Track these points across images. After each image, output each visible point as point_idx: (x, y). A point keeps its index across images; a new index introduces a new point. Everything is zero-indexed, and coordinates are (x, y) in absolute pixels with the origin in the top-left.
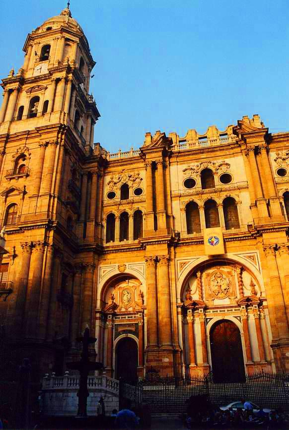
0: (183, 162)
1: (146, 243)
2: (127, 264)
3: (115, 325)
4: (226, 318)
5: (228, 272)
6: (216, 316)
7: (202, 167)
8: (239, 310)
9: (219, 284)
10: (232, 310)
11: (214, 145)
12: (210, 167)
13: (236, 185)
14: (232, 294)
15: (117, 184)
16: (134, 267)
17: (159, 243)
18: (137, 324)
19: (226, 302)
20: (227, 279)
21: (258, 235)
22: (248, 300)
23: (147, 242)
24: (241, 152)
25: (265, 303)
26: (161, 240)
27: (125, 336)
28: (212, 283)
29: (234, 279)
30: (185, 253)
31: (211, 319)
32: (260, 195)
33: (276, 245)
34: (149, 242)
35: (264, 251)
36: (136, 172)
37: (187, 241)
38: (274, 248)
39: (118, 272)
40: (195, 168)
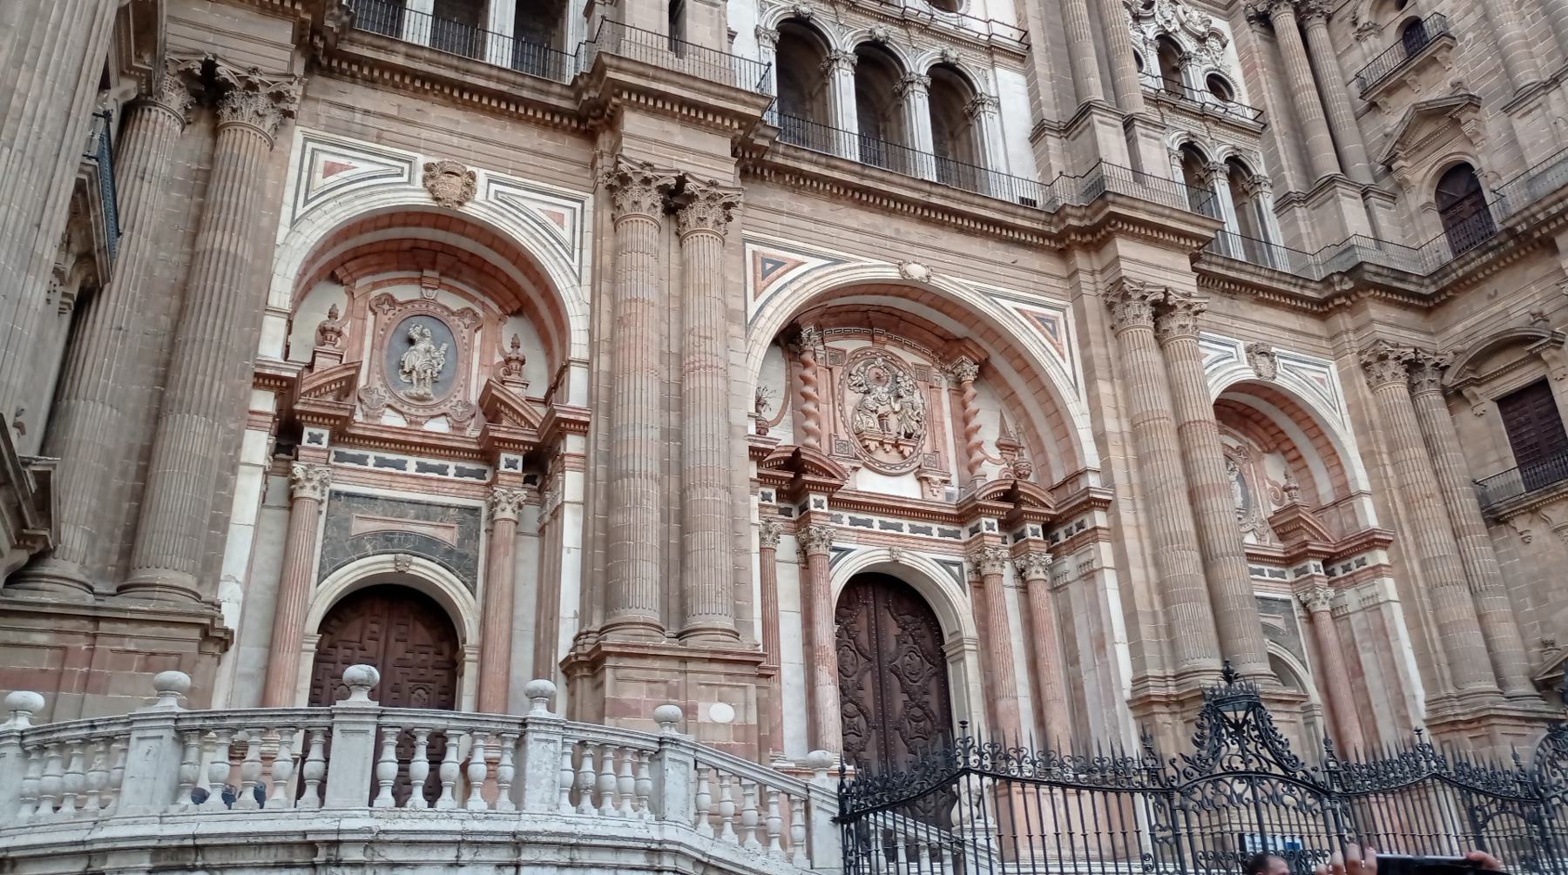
1: (632, 89)
2: (482, 175)
3: (337, 494)
4: (906, 559)
6: (866, 544)
8: (956, 535)
9: (881, 410)
10: (928, 531)
13: (981, 28)
16: (532, 206)
17: (694, 113)
18: (475, 511)
19: (906, 488)
21: (1089, 238)
22: (1010, 495)
23: (640, 91)
25: (1100, 518)
26: (711, 101)
27: (390, 568)
28: (852, 398)
29: (940, 404)
30: (785, 220)
32: (1096, 92)
33: (1166, 293)
34: (648, 93)
35: (1110, 307)
38: (1155, 304)
39: (420, 198)
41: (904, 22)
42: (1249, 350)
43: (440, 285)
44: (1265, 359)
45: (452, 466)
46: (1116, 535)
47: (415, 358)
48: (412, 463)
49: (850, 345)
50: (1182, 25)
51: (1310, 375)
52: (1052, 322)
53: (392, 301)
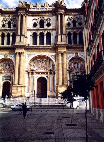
0: (33, 16)
5: (45, 60)
7: (40, 19)
11: (46, 10)
12: (43, 19)
14: (46, 68)
15: (6, 22)
20: (45, 63)
22: (51, 70)
24: (55, 15)
28: (39, 64)
29: (47, 63)
31: (37, 76)
33: (62, 52)
36: (14, 17)
37: (31, 48)
39: (4, 57)
40: (37, 19)
41: (44, 30)
42: (75, 53)
43: (9, 61)
44: (77, 54)
45: (10, 74)
46: (56, 73)
47: (7, 67)
48: (7, 74)
49: (39, 59)
50: (76, 18)
51: (82, 55)
52: (54, 55)
53: (5, 63)
